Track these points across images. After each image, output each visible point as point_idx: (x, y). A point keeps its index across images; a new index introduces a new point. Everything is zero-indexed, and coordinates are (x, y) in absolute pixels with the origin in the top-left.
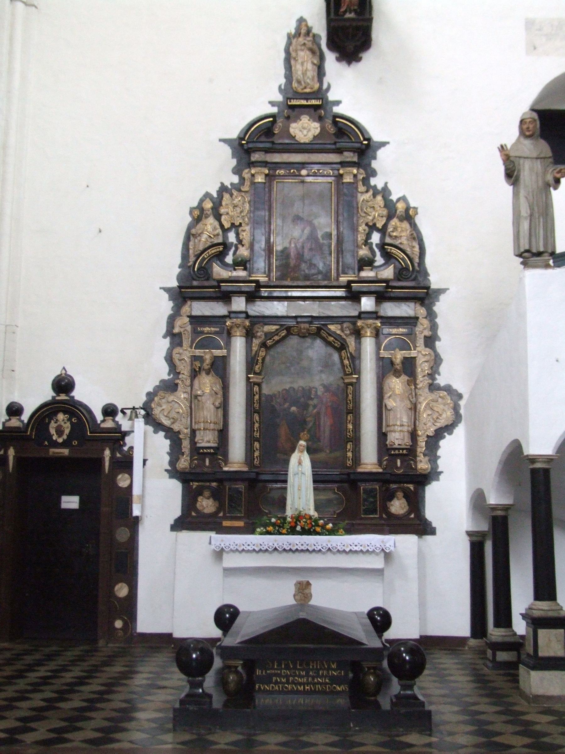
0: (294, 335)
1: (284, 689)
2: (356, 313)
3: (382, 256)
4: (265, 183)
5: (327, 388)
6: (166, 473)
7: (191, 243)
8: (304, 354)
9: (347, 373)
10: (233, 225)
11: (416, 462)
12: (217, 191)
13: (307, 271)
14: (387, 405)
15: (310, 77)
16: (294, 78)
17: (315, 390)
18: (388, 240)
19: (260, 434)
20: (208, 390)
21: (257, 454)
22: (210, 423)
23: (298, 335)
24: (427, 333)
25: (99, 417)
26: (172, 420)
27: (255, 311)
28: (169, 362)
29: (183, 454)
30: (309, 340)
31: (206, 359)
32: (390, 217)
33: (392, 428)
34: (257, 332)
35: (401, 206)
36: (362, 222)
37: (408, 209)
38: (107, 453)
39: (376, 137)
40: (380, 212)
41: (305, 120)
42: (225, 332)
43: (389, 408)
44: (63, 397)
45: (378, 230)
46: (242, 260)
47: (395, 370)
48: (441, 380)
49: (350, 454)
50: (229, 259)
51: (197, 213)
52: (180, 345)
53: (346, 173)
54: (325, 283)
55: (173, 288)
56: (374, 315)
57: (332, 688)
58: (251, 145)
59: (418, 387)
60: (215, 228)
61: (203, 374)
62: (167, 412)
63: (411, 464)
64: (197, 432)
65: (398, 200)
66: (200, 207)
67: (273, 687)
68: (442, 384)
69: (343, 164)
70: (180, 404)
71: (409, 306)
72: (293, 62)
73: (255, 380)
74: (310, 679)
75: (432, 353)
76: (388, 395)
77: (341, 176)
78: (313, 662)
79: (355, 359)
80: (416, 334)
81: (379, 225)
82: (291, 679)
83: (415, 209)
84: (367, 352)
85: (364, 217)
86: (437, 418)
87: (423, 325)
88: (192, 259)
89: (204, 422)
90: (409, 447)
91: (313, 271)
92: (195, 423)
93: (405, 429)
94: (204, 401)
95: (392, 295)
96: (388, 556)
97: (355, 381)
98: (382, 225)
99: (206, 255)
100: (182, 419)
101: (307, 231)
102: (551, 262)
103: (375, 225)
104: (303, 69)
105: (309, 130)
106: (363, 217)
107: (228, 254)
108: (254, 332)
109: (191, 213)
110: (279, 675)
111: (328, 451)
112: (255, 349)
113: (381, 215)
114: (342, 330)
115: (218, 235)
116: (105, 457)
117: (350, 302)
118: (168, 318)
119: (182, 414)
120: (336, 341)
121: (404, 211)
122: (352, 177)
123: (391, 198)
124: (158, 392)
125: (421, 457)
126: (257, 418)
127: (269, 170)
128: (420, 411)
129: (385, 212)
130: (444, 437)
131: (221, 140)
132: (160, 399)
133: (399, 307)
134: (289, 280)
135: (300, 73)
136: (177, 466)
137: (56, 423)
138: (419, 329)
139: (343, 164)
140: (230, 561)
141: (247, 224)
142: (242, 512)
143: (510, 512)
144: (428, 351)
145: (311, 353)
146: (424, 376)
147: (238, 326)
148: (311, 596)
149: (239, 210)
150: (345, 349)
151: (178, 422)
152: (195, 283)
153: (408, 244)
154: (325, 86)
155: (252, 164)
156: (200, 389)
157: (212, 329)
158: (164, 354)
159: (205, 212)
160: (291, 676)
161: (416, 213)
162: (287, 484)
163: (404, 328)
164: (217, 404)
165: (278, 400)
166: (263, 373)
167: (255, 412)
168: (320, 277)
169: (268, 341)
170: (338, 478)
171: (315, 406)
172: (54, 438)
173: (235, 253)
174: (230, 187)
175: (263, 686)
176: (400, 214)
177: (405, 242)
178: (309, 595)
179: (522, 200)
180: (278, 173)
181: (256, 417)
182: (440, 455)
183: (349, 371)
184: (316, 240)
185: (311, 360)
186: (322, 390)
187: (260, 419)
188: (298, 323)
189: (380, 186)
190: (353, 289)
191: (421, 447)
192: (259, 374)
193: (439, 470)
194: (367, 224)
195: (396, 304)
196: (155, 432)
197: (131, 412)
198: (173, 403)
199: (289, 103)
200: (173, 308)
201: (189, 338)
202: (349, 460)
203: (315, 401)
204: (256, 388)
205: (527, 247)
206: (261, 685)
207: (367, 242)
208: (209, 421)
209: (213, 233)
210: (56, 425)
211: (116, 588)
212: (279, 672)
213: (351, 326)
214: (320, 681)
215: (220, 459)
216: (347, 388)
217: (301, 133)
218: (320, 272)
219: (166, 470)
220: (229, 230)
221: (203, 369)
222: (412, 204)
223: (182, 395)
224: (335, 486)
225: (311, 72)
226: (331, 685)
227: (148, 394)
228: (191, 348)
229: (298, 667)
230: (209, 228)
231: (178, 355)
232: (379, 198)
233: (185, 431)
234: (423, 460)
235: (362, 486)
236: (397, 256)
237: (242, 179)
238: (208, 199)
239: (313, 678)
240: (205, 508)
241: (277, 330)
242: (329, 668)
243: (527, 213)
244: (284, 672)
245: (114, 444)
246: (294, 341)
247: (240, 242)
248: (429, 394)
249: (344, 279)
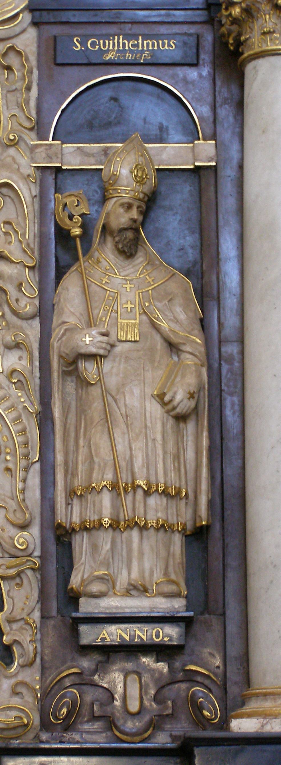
22: (147, 493)
89: (114, 487)
201: (28, 89)
208: (141, 482)
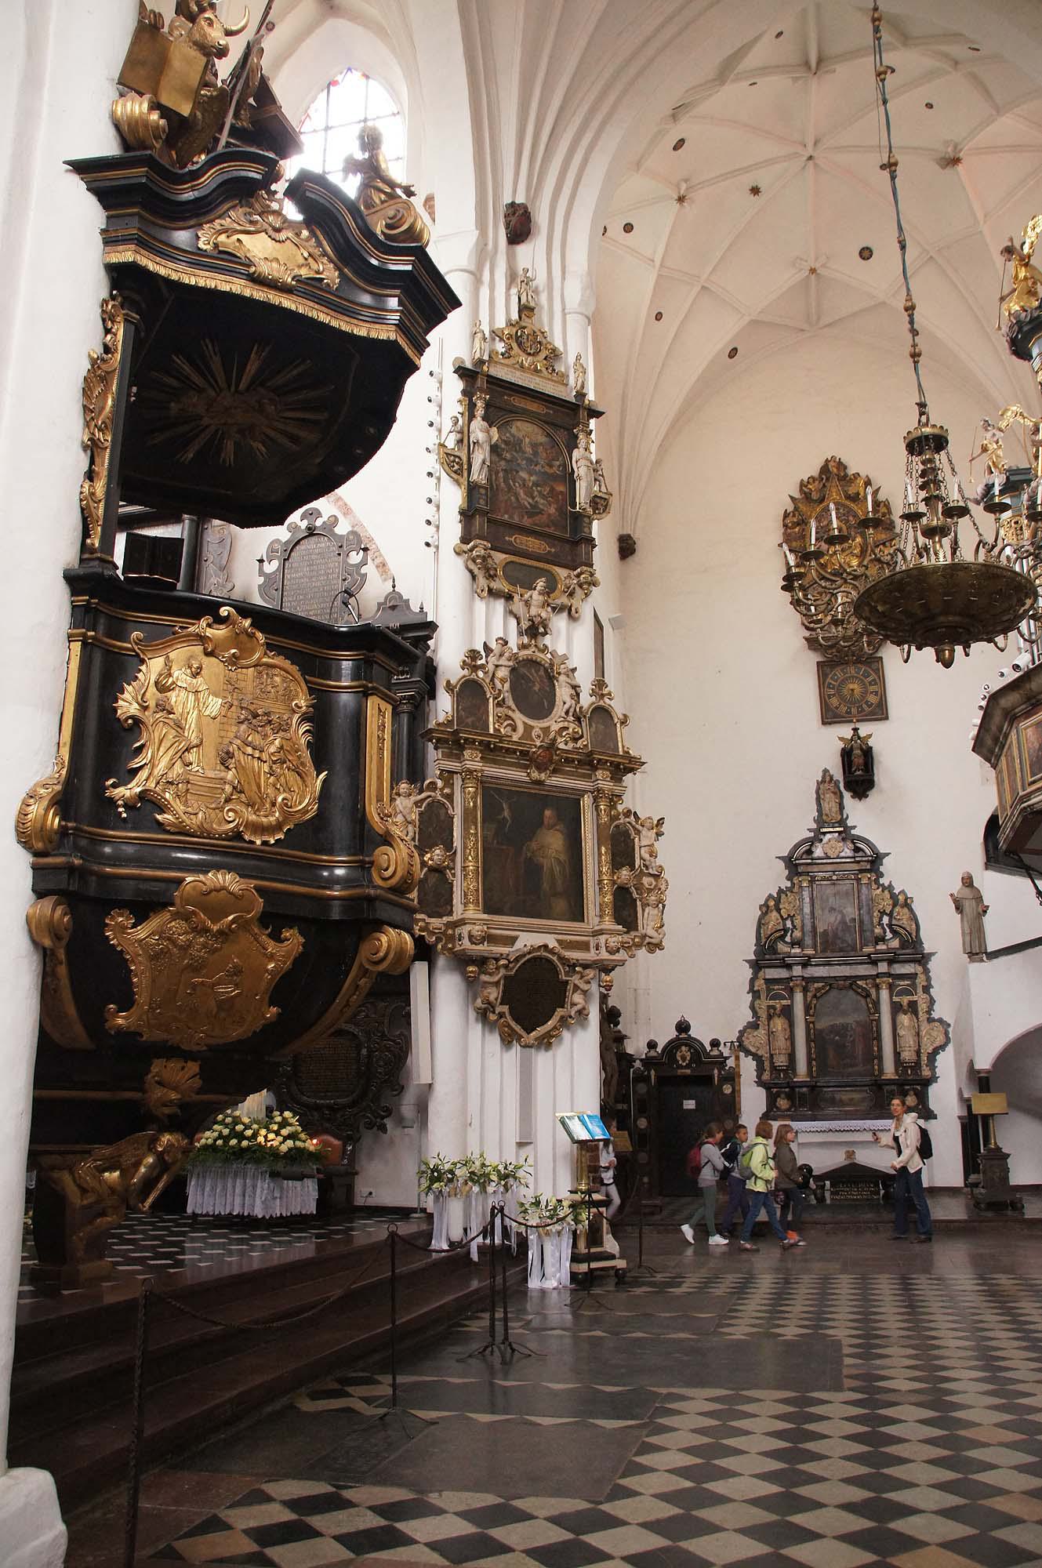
18: (894, 922)
21: (814, 1069)
24: (925, 984)
25: (708, 1048)
32: (894, 906)
38: (716, 1071)
44: (683, 1035)
45: (886, 914)
48: (935, 1015)
49: (876, 1067)
50: (788, 939)
65: (899, 893)
66: (766, 906)
72: (822, 801)
79: (877, 1004)
81: (888, 912)
88: (763, 940)
91: (845, 945)
101: (839, 918)
102: (985, 958)
109: (760, 909)
112: (809, 999)
114: (866, 984)
139: (861, 871)
144: (925, 996)
147: (797, 985)
152: (767, 957)
154: (845, 817)
155: (800, 874)
170: (869, 1083)
179: (966, 923)
189: (886, 885)
192: (813, 1016)
196: (746, 1057)
204: (811, 1025)
207: (880, 924)
220: (786, 919)
223: (762, 1032)
224: (867, 1088)
225: (835, 809)
227: (740, 1032)
232: (886, 892)
237: (793, 884)
246: (834, 993)
247: (794, 927)
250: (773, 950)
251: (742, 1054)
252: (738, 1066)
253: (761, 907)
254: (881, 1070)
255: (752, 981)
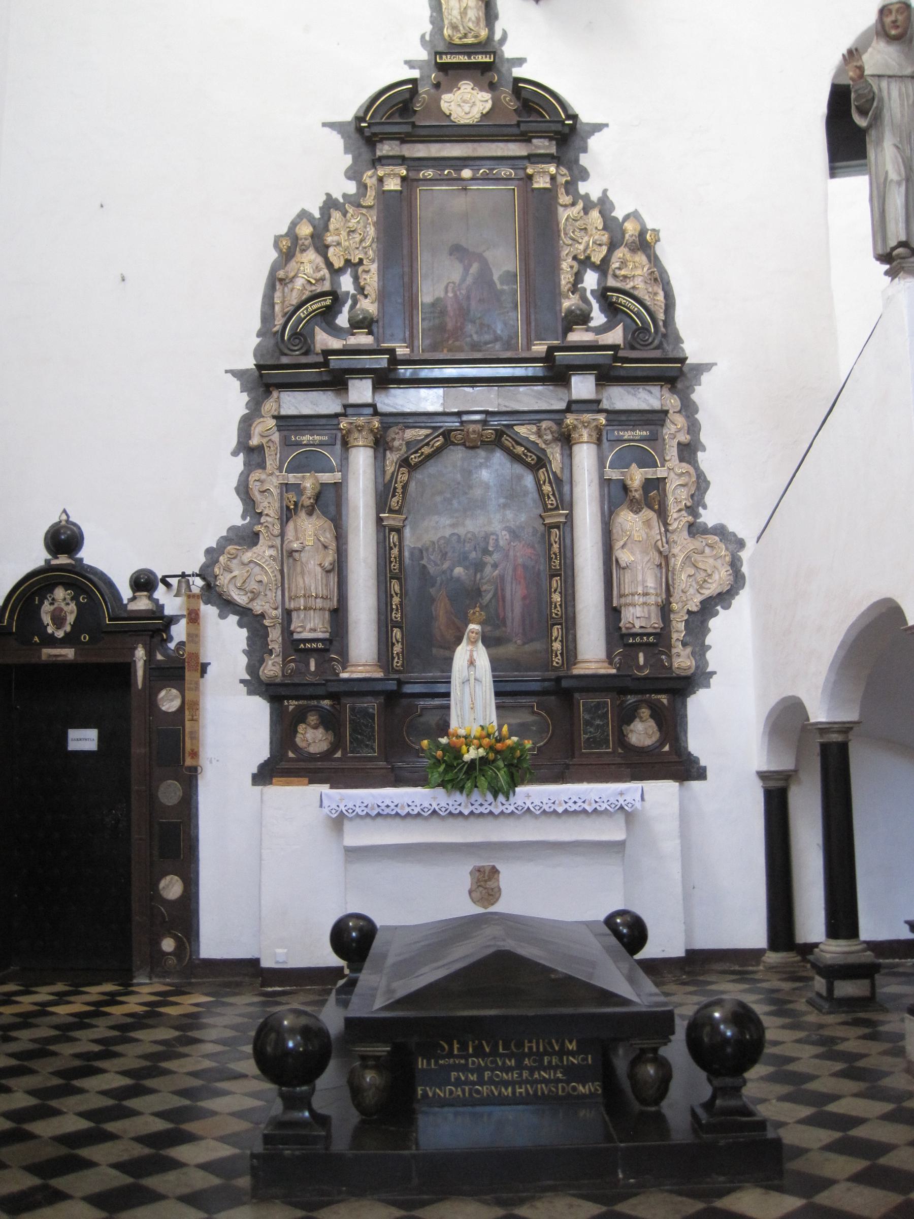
0: (457, 445)
1: (474, 1095)
2: (562, 406)
3: (602, 310)
4: (401, 192)
5: (514, 534)
6: (242, 685)
7: (278, 295)
8: (475, 476)
9: (549, 506)
10: (348, 262)
11: (670, 657)
12: (321, 209)
13: (475, 337)
14: (620, 560)
15: (474, 18)
16: (446, 22)
17: (494, 537)
18: (611, 282)
19: (402, 614)
20: (310, 541)
21: (397, 648)
22: (316, 598)
23: (464, 444)
24: (684, 438)
25: (126, 593)
26: (249, 594)
27: (388, 405)
28: (242, 496)
29: (270, 652)
30: (482, 453)
31: (305, 488)
33: (629, 600)
34: (394, 439)
35: (631, 228)
36: (567, 255)
37: (642, 233)
39: (586, 117)
40: (596, 237)
41: (466, 88)
42: (339, 442)
43: (623, 564)
44: (63, 560)
45: (595, 267)
46: (365, 318)
47: (631, 500)
48: (709, 517)
49: (557, 646)
50: (342, 320)
51: (285, 243)
52: (262, 465)
53: (539, 172)
54: (508, 355)
55: (247, 370)
56: (592, 406)
57: (569, 1089)
58: (376, 129)
59: (670, 528)
60: (317, 268)
61: (303, 514)
62: (241, 582)
63: (662, 660)
64: (294, 615)
65: (627, 218)
67: (451, 1092)
68: (710, 525)
69: (532, 158)
70: (263, 568)
71: (651, 393)
73: (391, 522)
74: (525, 1074)
75: (692, 470)
76: (622, 543)
77: (530, 177)
78: (530, 1042)
80: (664, 440)
82: (487, 1074)
83: (656, 232)
84: (583, 468)
85: (571, 245)
86: (705, 581)
87: (676, 425)
88: (279, 321)
89: (305, 596)
90: (658, 631)
91: (487, 337)
92: (290, 598)
93: (652, 600)
94: (304, 560)
95: (622, 373)
96: (628, 816)
97: (563, 520)
98: (600, 259)
99: (302, 312)
100: (268, 593)
103: (588, 258)
104: (460, 6)
105: (474, 104)
106: (568, 245)
107: (340, 312)
108: (388, 439)
109: (276, 245)
110: (464, 1068)
111: (519, 642)
112: (390, 469)
113: (598, 242)
114: (539, 434)
115: (323, 279)
116: (137, 660)
117: (551, 387)
118: (240, 422)
119: (267, 584)
120: (529, 454)
121: (637, 234)
122: (548, 179)
123: (613, 214)
124: (225, 548)
125: (678, 648)
126: (397, 588)
127: (408, 170)
128: (674, 569)
129: (605, 238)
130: (717, 614)
131: (324, 125)
132: (230, 559)
133: (635, 395)
134: (445, 351)
135: (456, 13)
136: (260, 673)
137: (52, 604)
138: (669, 429)
139: (532, 158)
140: (357, 836)
141: (373, 261)
142: (373, 749)
143: (851, 736)
144: (685, 467)
145: (485, 475)
146: (680, 510)
147: (359, 428)
148: (500, 890)
149: (358, 238)
150: (544, 466)
151: (261, 597)
152: (285, 360)
153: (646, 289)
154: (498, 36)
155: (377, 162)
156: (297, 539)
157: (317, 438)
158: (235, 484)
159: (300, 242)
160: (487, 1068)
161: (658, 240)
162: (450, 700)
163: (644, 430)
164: (327, 564)
165: (432, 557)
166: (405, 510)
167: (391, 578)
168: (498, 346)
169: (413, 456)
171: (495, 566)
172: (50, 630)
173: (353, 306)
174: (341, 200)
175: (431, 1089)
176: (631, 240)
177: (641, 286)
178: (496, 890)
180: (423, 174)
181: (396, 586)
182: (710, 644)
183: (552, 504)
184: (491, 284)
185: (487, 487)
186: (507, 537)
187: (401, 590)
188: (462, 422)
189: (595, 196)
190: (557, 363)
191: (677, 631)
192: (398, 512)
193: (709, 670)
194: (575, 258)
195: (629, 389)
196: (222, 616)
197: (179, 582)
198: (252, 565)
199: (438, 61)
200: (247, 404)
201: (276, 454)
202: (556, 656)
203: (496, 557)
204: (394, 537)
205: (903, 238)
206: (428, 1089)
207: (575, 286)
208: (314, 594)
209: (314, 276)
210: (52, 608)
211: (163, 884)
212: (463, 1061)
213: (555, 427)
214: (544, 1077)
215: (334, 660)
216: (550, 534)
217: (459, 109)
218: (497, 339)
219: (242, 681)
221: (302, 506)
222: (650, 226)
223: (264, 551)
224: (532, 701)
226: (568, 1083)
227: (209, 551)
228: (281, 472)
229: (501, 1050)
230: (309, 269)
231: (258, 483)
232: (595, 214)
233: (274, 613)
234: (682, 653)
235: (582, 701)
236: (629, 309)
237: (363, 187)
238: (305, 220)
239: (532, 1070)
240: (309, 744)
241: (427, 436)
242: (563, 1052)
243: (899, 174)
244: (473, 1063)
245: (152, 637)
246: (456, 456)
247: (361, 290)
248: (689, 540)
249: (540, 348)
250: (302, 338)
251: (209, 612)
252: (194, 636)
253: (277, 240)
254: (571, 652)
255: (246, 424)
